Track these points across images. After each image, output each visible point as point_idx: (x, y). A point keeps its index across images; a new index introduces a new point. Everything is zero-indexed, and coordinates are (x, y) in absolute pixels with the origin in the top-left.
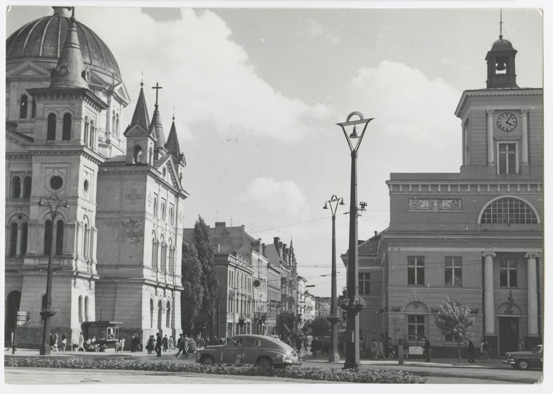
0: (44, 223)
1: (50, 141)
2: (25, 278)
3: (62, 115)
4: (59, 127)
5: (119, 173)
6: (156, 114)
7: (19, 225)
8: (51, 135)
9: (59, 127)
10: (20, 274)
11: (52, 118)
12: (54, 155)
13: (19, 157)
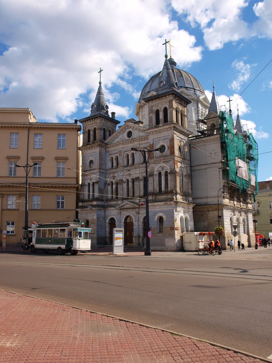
3: (162, 109)
4: (161, 116)
8: (158, 122)
9: (161, 116)
11: (157, 112)
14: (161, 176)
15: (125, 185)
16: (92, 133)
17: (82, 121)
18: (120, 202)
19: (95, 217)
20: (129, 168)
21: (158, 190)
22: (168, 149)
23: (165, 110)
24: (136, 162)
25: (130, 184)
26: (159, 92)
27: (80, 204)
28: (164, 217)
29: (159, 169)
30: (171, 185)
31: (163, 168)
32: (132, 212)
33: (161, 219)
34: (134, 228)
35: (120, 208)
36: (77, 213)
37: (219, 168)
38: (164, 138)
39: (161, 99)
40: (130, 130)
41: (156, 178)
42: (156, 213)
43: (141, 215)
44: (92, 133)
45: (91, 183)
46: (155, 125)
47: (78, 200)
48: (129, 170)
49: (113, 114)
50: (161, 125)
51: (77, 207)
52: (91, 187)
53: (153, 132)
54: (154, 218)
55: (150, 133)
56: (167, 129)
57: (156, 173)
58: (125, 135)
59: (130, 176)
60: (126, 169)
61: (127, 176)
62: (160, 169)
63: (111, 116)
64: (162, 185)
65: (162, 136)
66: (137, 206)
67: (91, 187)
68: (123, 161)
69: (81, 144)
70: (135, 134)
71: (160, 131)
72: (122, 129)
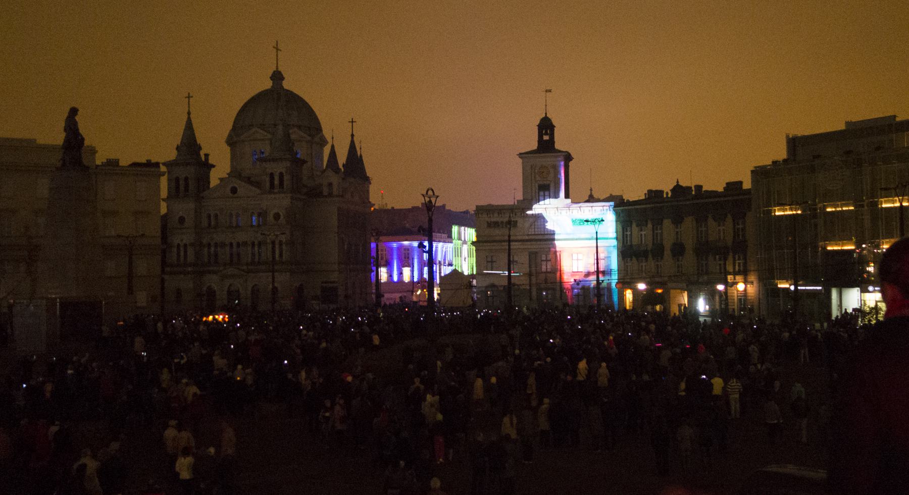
3: (277, 174)
4: (276, 182)
6: (352, 142)
16: (182, 182)
17: (164, 164)
18: (221, 268)
19: (191, 285)
21: (271, 259)
27: (168, 269)
36: (163, 281)
44: (182, 182)
45: (182, 244)
47: (164, 263)
48: (233, 233)
49: (207, 155)
50: (276, 191)
51: (163, 271)
52: (182, 249)
58: (228, 189)
63: (203, 159)
66: (245, 274)
67: (182, 249)
69: (164, 193)
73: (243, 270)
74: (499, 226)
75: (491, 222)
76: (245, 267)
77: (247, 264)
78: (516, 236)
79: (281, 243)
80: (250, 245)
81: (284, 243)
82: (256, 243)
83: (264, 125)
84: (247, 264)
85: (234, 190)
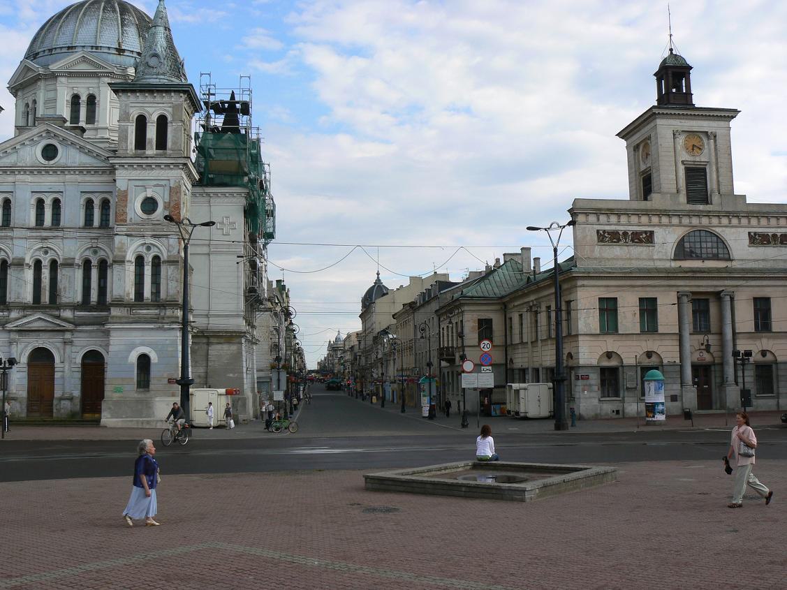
0: (133, 260)
1: (139, 151)
2: (112, 333)
3: (155, 118)
4: (151, 133)
5: (208, 194)
7: (94, 262)
8: (141, 142)
9: (151, 133)
10: (108, 326)
11: (141, 122)
12: (144, 169)
13: (108, 172)
14: (144, 266)
15: (29, 275)
18: (14, 314)
20: (45, 234)
21: (132, 296)
22: (165, 208)
23: (162, 122)
24: (65, 219)
25: (46, 273)
26: (147, 77)
28: (154, 357)
29: (140, 249)
30: (170, 287)
31: (149, 248)
32: (51, 340)
33: (144, 361)
34: (56, 377)
35: (18, 328)
37: (238, 257)
38: (155, 182)
39: (155, 95)
40: (53, 142)
41: (131, 269)
42: (133, 346)
43: (79, 348)
46: (134, 148)
48: (46, 239)
53: (131, 165)
54: (127, 357)
55: (122, 165)
56: (167, 165)
57: (130, 256)
58: (38, 150)
59: (46, 253)
60: (34, 234)
61: (37, 253)
62: (143, 250)
64: (143, 284)
65: (152, 178)
66: (71, 327)
68: (25, 214)
70: (66, 156)
71: (149, 165)
72: (31, 135)
73: (66, 320)
74: (619, 240)
75: (604, 231)
76: (67, 314)
77: (75, 307)
78: (653, 260)
79: (157, 262)
80: (79, 266)
81: (165, 262)
82: (94, 262)
83: (97, 48)
84: (75, 307)
85: (50, 152)
